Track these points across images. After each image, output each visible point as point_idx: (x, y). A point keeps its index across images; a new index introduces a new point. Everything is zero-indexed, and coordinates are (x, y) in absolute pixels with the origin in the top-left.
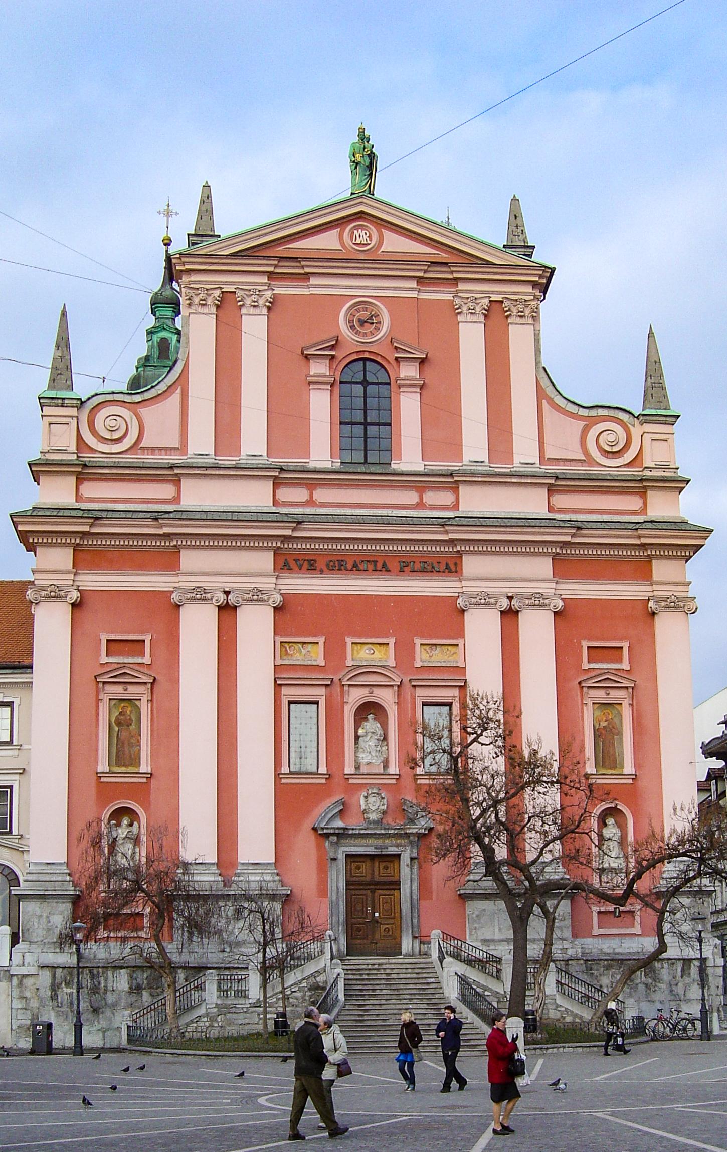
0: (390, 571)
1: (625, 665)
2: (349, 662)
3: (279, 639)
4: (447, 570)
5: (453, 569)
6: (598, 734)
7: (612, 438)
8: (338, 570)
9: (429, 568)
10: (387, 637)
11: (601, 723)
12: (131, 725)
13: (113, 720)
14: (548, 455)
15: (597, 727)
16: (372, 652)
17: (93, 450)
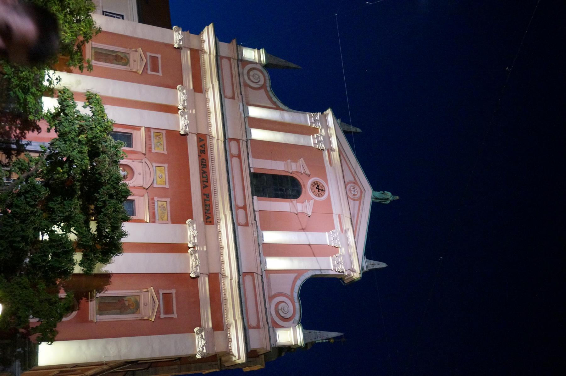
0: (204, 188)
1: (162, 316)
2: (154, 164)
3: (164, 132)
4: (207, 217)
5: (208, 220)
6: (120, 299)
7: (286, 309)
8: (202, 165)
9: (207, 208)
10: (170, 184)
11: (127, 302)
12: (116, 61)
13: (119, 54)
14: (272, 275)
15: (124, 299)
16: (160, 177)
17: (243, 68)
